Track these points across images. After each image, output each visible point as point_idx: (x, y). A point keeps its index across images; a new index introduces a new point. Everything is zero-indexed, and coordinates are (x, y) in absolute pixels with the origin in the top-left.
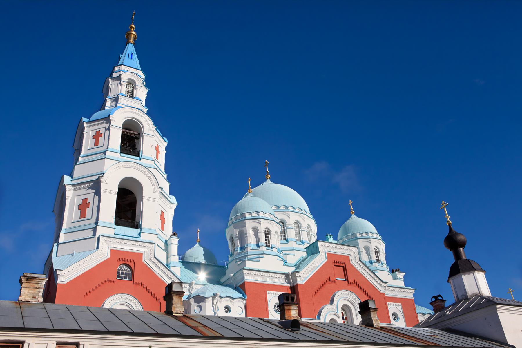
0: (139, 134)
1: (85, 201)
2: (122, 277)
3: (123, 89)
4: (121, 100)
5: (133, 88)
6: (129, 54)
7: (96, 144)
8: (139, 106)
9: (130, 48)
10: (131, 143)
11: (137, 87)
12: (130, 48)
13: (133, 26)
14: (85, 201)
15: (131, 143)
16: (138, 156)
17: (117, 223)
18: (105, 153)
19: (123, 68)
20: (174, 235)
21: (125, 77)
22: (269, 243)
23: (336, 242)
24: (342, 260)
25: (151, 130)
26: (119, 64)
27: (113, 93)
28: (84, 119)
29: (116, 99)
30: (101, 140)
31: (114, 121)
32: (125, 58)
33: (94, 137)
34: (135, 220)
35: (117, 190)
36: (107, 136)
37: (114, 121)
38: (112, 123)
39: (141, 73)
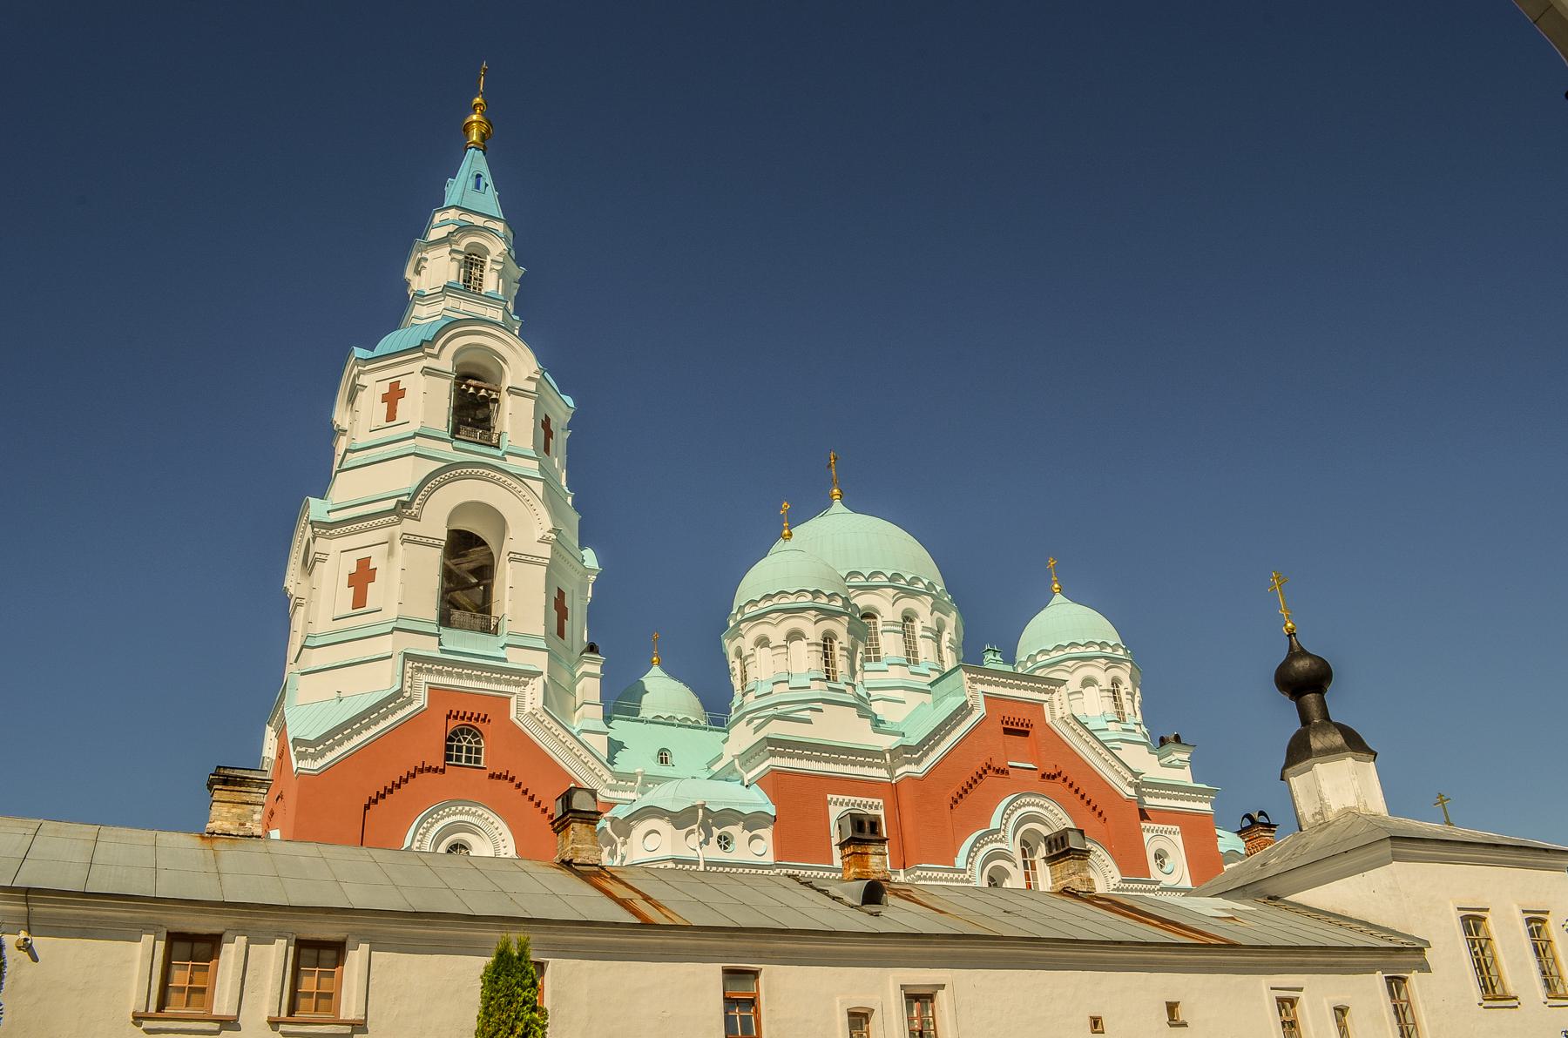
1: (364, 563)
2: (459, 759)
7: (391, 416)
8: (498, 316)
9: (474, 162)
10: (473, 410)
12: (474, 162)
14: (364, 563)
15: (473, 410)
17: (445, 620)
20: (592, 648)
22: (834, 672)
23: (1009, 668)
24: (1024, 715)
25: (530, 379)
28: (359, 352)
32: (456, 189)
33: (385, 398)
34: (488, 611)
35: (443, 535)
39: (500, 227)
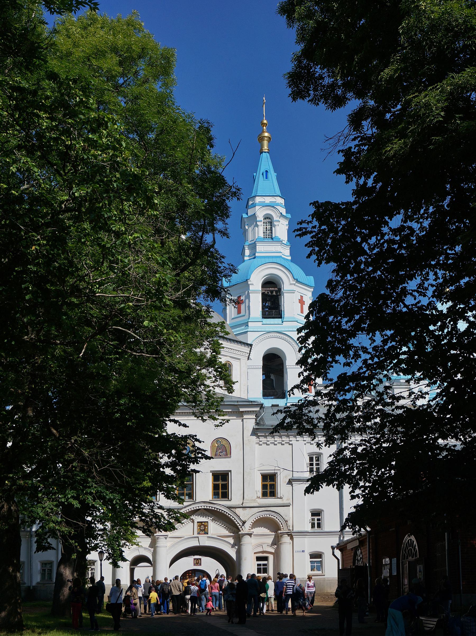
0: (280, 290)
3: (260, 231)
4: (260, 248)
5: (271, 223)
6: (263, 174)
11: (275, 223)
12: (265, 162)
13: (265, 122)
16: (281, 317)
18: (246, 324)
19: (258, 200)
21: (260, 213)
26: (253, 195)
27: (250, 237)
29: (253, 247)
30: (243, 306)
31: (252, 284)
36: (247, 305)
37: (252, 284)
38: (251, 288)
